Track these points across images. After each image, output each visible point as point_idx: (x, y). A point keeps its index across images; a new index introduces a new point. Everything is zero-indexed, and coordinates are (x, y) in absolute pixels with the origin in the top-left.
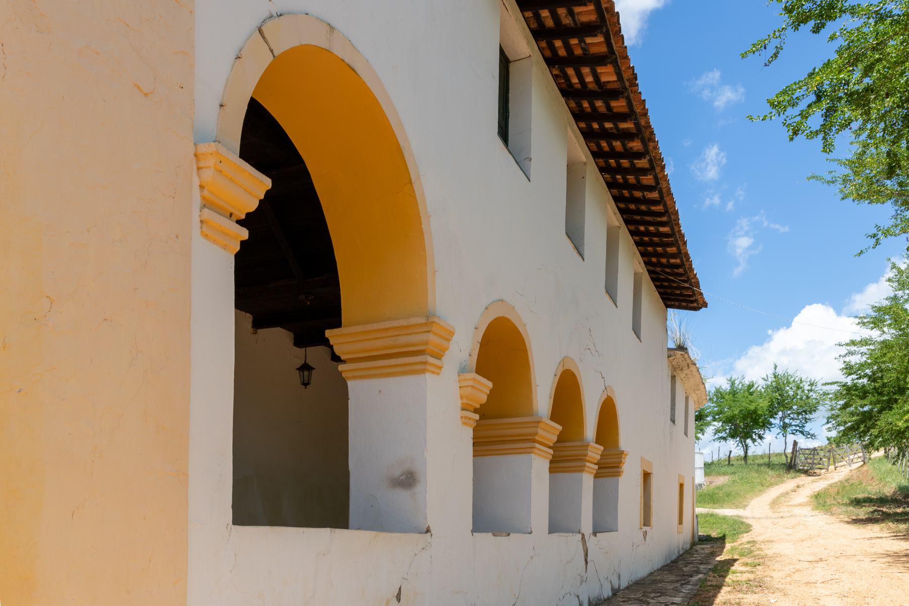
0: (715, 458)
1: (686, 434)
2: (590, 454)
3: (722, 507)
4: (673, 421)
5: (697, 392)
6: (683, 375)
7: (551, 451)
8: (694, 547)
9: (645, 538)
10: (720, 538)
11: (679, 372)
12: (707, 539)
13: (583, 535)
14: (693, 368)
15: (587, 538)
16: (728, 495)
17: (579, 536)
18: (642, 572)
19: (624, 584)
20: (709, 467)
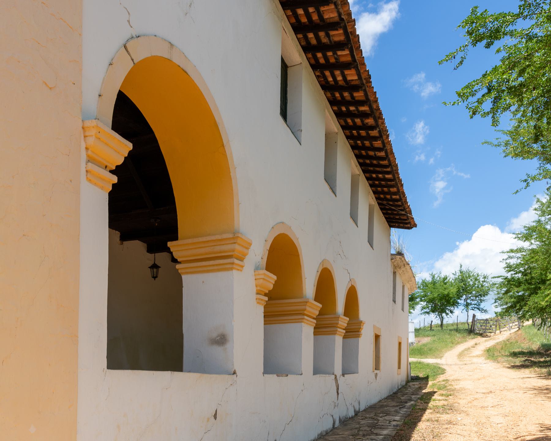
0: (422, 326)
1: (403, 310)
2: (340, 322)
3: (426, 357)
4: (394, 301)
5: (410, 282)
6: (401, 272)
7: (315, 321)
8: (408, 384)
9: (376, 378)
10: (425, 378)
11: (398, 269)
12: (416, 379)
13: (336, 376)
14: (407, 267)
15: (338, 377)
16: (430, 350)
17: (333, 377)
18: (374, 400)
19: (362, 408)
20: (417, 331)
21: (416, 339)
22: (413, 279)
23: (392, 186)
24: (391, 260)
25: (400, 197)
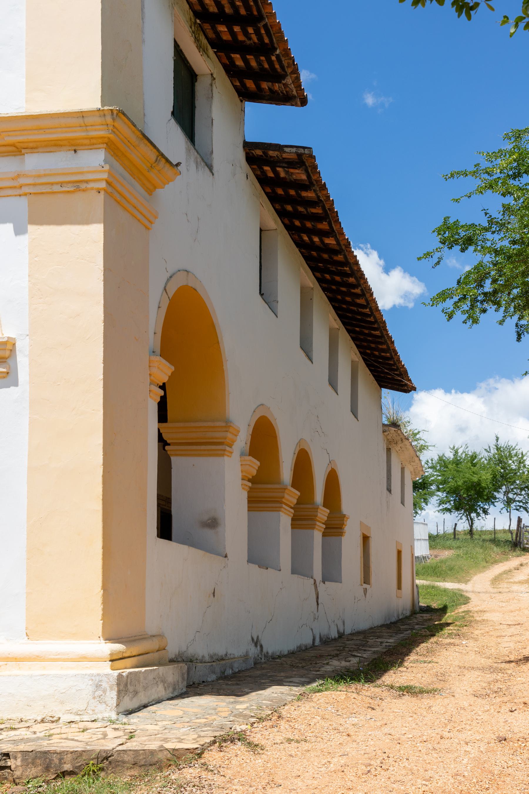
0: (441, 532)
1: (403, 503)
2: (319, 515)
3: (444, 580)
4: (389, 490)
5: (412, 464)
6: (398, 448)
7: (292, 511)
8: (414, 615)
9: (365, 594)
10: (440, 609)
11: (394, 445)
12: (428, 609)
13: (315, 580)
14: (406, 442)
15: (318, 583)
16: (451, 569)
17: (312, 581)
18: (364, 625)
19: (348, 631)
20: (433, 539)
21: (432, 551)
22: (416, 459)
23: (382, 343)
24: (383, 432)
25: (391, 354)
